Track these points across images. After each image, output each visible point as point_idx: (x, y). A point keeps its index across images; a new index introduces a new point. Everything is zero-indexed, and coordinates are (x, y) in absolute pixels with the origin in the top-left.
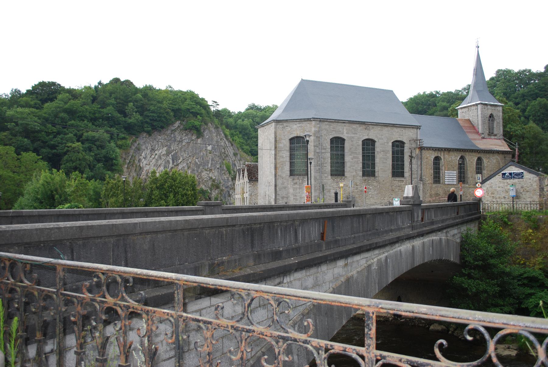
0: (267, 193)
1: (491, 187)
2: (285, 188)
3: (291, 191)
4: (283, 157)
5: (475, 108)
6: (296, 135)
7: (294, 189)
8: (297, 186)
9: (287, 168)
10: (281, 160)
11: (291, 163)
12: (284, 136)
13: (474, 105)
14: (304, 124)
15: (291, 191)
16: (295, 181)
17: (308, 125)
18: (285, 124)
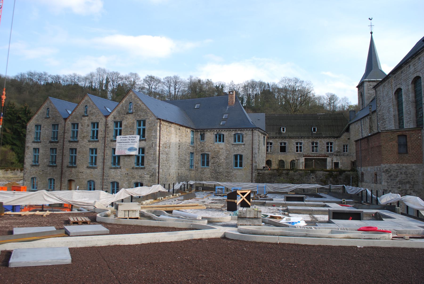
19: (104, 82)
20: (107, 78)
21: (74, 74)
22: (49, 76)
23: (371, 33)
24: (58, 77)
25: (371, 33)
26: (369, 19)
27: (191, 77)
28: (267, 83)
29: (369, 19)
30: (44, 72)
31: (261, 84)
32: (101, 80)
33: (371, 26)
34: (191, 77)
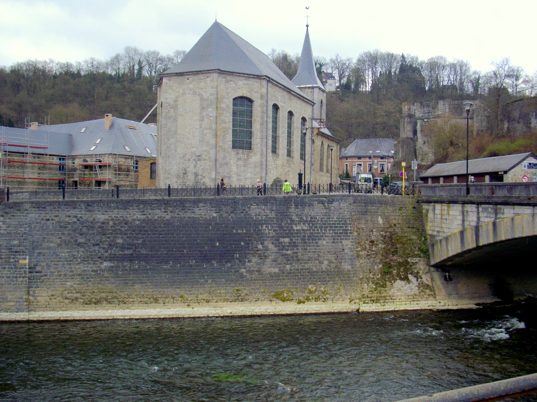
0: (191, 169)
1: (515, 175)
2: (227, 164)
3: (234, 168)
4: (225, 122)
5: (310, 90)
6: (241, 95)
7: (238, 166)
8: (241, 163)
9: (229, 137)
10: (223, 125)
11: (234, 131)
12: (227, 93)
13: (309, 88)
14: (252, 81)
15: (234, 168)
16: (240, 156)
17: (256, 84)
18: (229, 78)
19: (137, 67)
20: (140, 61)
21: (92, 59)
22: (57, 64)
23: (307, 26)
24: (68, 65)
25: (307, 26)
26: (306, 8)
27: (274, 51)
28: (401, 54)
29: (306, 8)
30: (50, 59)
31: (390, 57)
32: (132, 65)
33: (307, 17)
34: (274, 51)
